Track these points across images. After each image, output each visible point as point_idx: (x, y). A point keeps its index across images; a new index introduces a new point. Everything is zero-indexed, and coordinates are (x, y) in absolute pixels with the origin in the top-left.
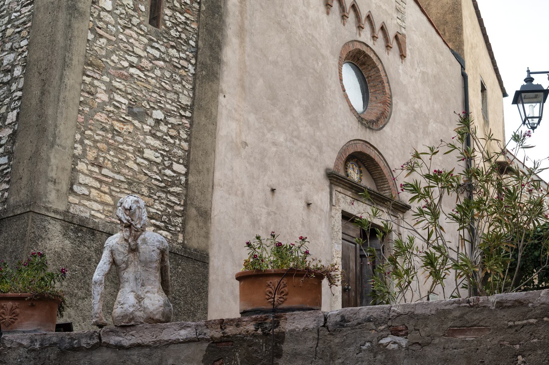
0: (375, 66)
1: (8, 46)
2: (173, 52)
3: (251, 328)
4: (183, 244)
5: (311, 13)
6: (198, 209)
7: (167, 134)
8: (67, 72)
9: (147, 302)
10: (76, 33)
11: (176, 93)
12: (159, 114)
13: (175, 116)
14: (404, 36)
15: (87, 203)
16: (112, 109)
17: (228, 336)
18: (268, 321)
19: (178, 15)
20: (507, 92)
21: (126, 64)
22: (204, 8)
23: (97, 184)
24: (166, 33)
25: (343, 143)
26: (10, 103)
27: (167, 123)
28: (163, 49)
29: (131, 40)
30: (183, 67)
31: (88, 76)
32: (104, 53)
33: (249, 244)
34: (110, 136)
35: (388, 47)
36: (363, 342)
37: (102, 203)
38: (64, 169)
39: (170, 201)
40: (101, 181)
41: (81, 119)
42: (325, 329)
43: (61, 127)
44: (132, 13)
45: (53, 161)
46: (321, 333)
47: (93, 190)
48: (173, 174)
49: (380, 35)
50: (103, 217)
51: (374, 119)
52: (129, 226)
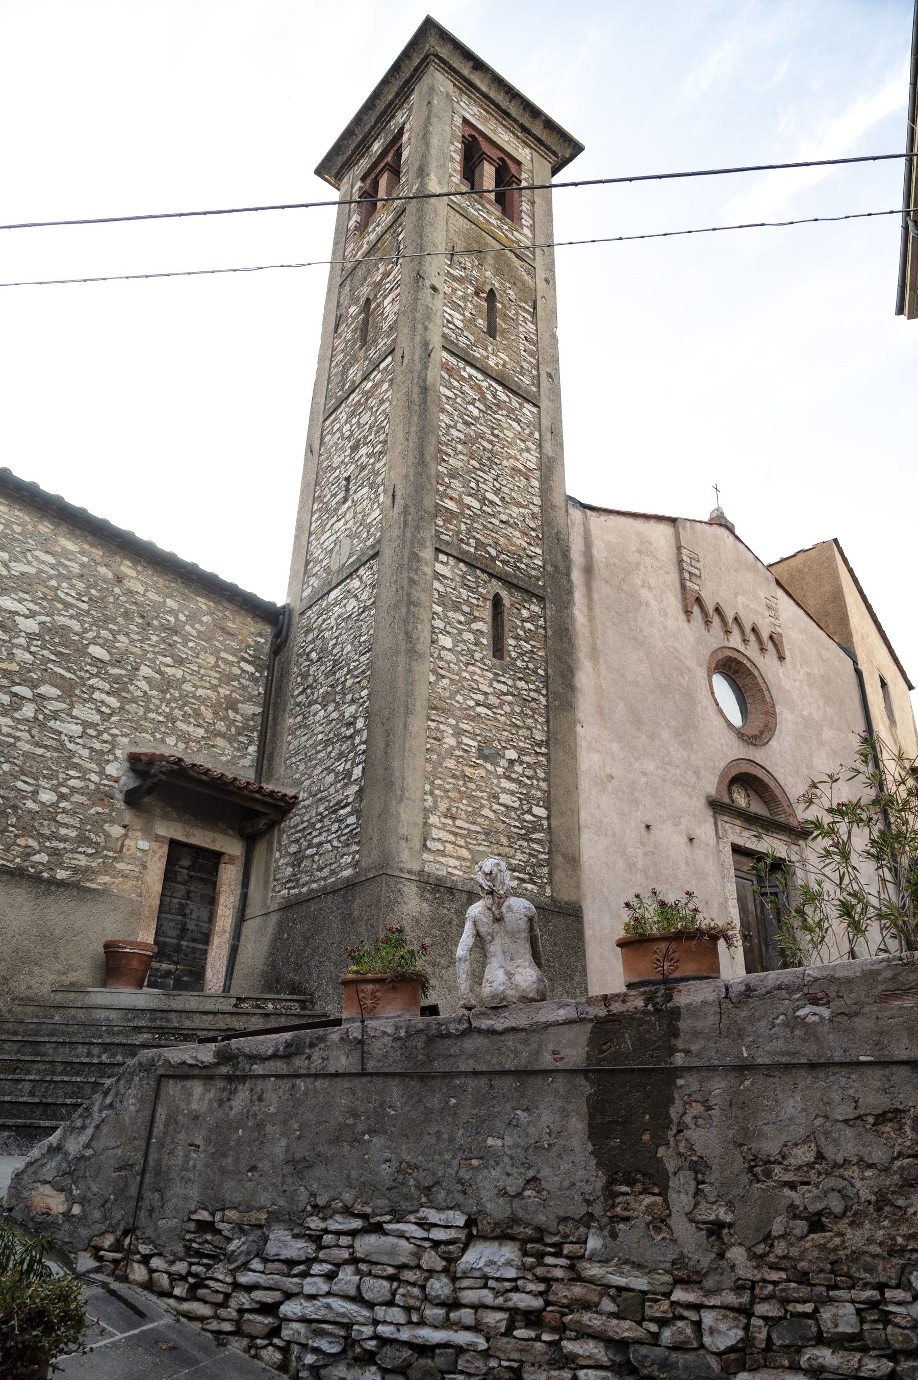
0: (750, 673)
1: (349, 697)
2: (521, 684)
3: (640, 1003)
4: (552, 897)
5: (670, 623)
6: (565, 856)
7: (523, 775)
8: (411, 719)
9: (518, 979)
10: (417, 677)
11: (529, 728)
12: (512, 754)
13: (529, 754)
14: (780, 635)
15: (443, 860)
16: (461, 753)
17: (614, 1015)
18: (659, 994)
19: (523, 643)
20: (914, 684)
21: (472, 703)
22: (550, 633)
23: (452, 838)
24: (513, 664)
25: (723, 765)
26: (354, 758)
27: (521, 763)
28: (510, 682)
29: (476, 677)
30: (533, 699)
31: (433, 721)
32: (447, 694)
33: (627, 905)
34: (461, 783)
35: (763, 650)
36: (775, 1015)
37: (459, 858)
38: (415, 824)
39: (533, 849)
40: (455, 834)
41: (429, 767)
42: (727, 1001)
43: (409, 779)
44: (474, 648)
45: (403, 816)
46: (723, 1006)
47: (447, 845)
48: (533, 819)
49: (752, 637)
50: (461, 873)
51: (757, 733)
52: (491, 893)
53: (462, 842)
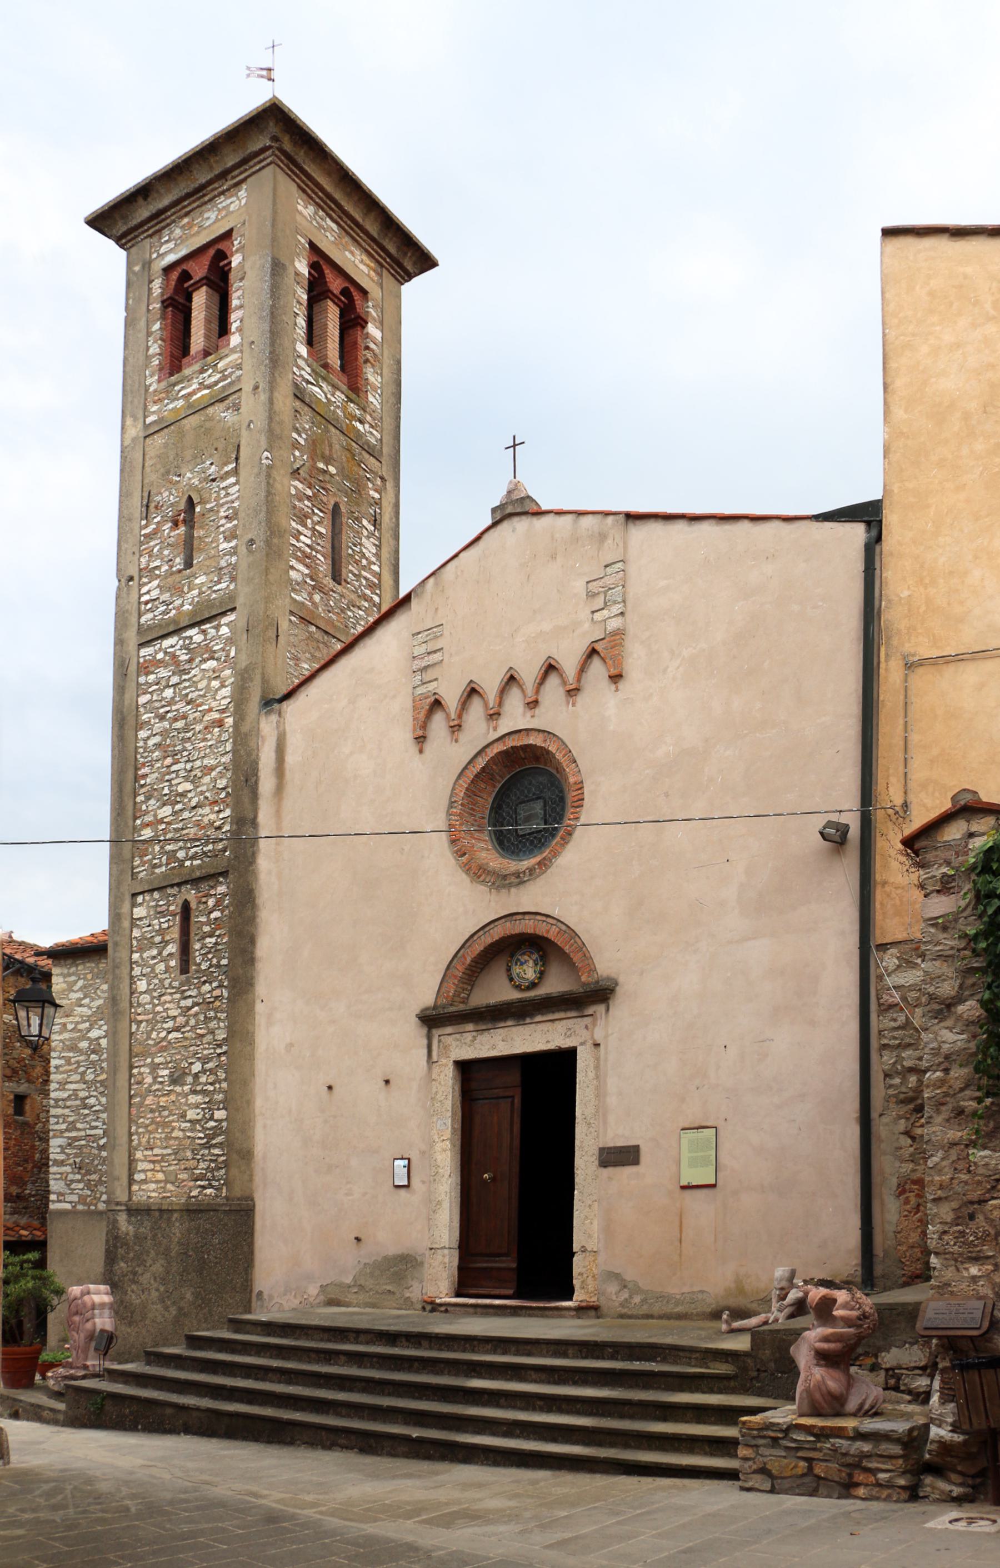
6: (239, 1152)
12: (197, 1067)
21: (163, 1034)
23: (151, 1166)
37: (157, 1182)
40: (153, 1162)
53: (158, 1168)
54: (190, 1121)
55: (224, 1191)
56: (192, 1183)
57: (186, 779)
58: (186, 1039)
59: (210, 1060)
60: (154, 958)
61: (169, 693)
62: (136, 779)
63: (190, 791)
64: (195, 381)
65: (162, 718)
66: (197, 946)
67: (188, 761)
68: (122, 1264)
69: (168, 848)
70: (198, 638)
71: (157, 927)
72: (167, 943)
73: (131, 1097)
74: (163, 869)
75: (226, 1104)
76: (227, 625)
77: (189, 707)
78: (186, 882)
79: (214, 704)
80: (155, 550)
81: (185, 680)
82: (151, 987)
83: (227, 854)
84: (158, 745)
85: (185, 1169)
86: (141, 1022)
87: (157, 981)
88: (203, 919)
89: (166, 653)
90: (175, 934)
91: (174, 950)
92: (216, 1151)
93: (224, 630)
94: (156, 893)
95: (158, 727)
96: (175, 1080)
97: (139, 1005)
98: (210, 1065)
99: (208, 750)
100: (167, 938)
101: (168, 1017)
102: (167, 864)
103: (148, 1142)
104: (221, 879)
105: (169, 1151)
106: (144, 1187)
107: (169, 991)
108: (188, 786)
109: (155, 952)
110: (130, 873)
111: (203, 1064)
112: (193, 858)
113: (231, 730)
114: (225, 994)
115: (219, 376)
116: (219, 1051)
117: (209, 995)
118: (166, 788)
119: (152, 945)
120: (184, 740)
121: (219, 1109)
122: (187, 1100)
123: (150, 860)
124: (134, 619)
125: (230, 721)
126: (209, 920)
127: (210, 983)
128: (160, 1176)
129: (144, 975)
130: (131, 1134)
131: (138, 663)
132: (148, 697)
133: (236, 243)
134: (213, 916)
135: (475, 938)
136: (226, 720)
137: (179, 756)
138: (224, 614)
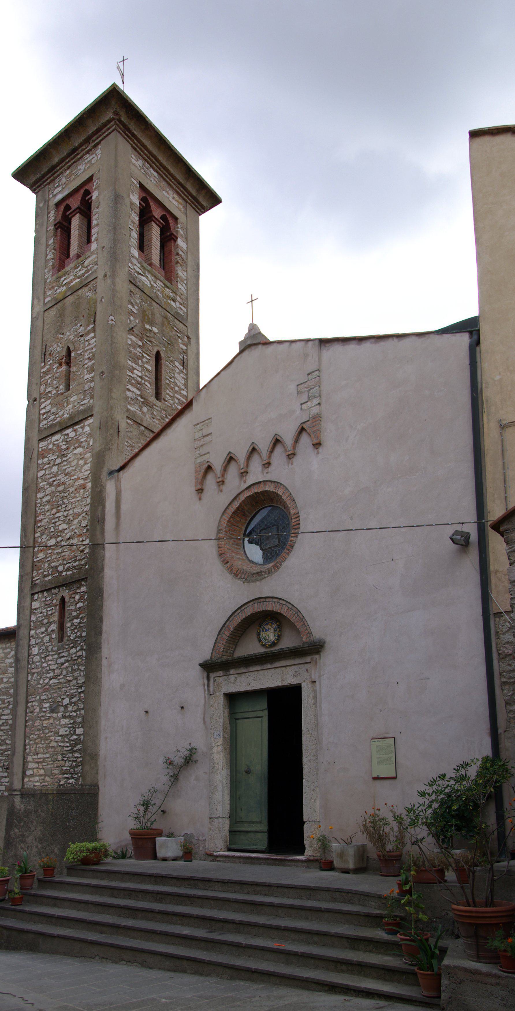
12: (66, 701)
21: (47, 681)
23: (37, 765)
37: (40, 776)
40: (38, 763)
53: (41, 767)
54: (61, 736)
55: (80, 780)
56: (61, 776)
57: (64, 522)
58: (60, 683)
59: (75, 696)
60: (43, 633)
61: (55, 469)
62: (36, 522)
63: (66, 529)
64: (72, 274)
65: (51, 485)
66: (69, 625)
67: (65, 511)
68: (16, 830)
69: (53, 564)
70: (72, 435)
71: (45, 614)
72: (51, 623)
73: (26, 721)
74: (50, 578)
75: (83, 724)
76: (89, 426)
77: (66, 477)
78: (63, 585)
79: (80, 475)
80: (49, 381)
81: (64, 461)
82: (41, 651)
83: (87, 567)
84: (48, 501)
85: (57, 767)
86: (34, 673)
87: (44, 648)
88: (73, 608)
89: (54, 445)
90: (56, 618)
91: (55, 628)
92: (77, 755)
93: (87, 429)
94: (45, 592)
95: (49, 490)
96: (52, 711)
97: (33, 662)
98: (74, 700)
99: (77, 503)
100: (51, 620)
101: (50, 670)
102: (52, 574)
103: (36, 750)
104: (83, 583)
105: (48, 755)
106: (32, 779)
107: (51, 653)
108: (65, 526)
109: (43, 629)
110: (31, 580)
111: (70, 699)
112: (67, 570)
113: (90, 490)
114: (84, 655)
115: (85, 269)
116: (80, 690)
117: (74, 655)
118: (52, 528)
119: (43, 625)
120: (63, 498)
121: (79, 728)
122: (60, 722)
123: (42, 573)
124: (37, 425)
125: (89, 485)
126: (76, 608)
127: (76, 648)
128: (42, 772)
129: (37, 644)
130: (25, 745)
131: (38, 451)
132: (43, 472)
133: (95, 184)
134: (78, 605)
135: (236, 614)
136: (87, 485)
137: (60, 508)
138: (86, 418)
